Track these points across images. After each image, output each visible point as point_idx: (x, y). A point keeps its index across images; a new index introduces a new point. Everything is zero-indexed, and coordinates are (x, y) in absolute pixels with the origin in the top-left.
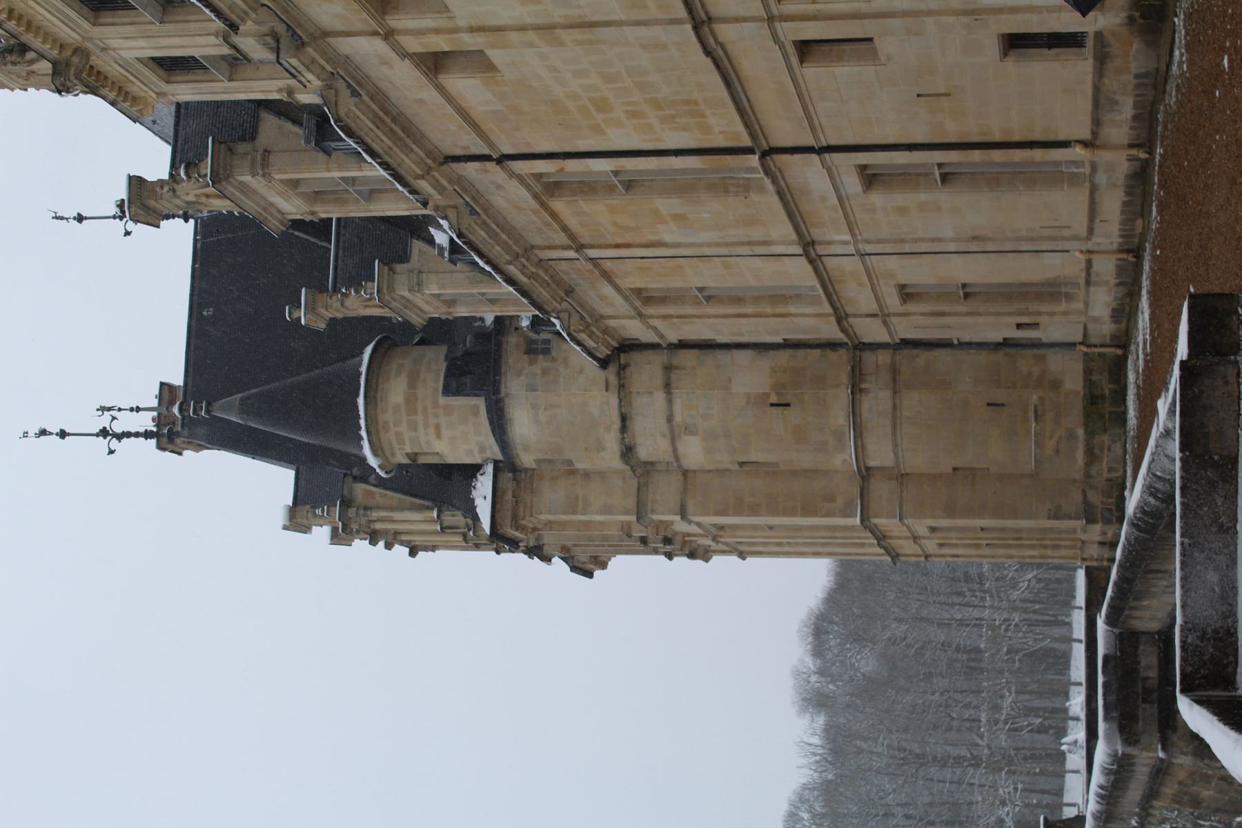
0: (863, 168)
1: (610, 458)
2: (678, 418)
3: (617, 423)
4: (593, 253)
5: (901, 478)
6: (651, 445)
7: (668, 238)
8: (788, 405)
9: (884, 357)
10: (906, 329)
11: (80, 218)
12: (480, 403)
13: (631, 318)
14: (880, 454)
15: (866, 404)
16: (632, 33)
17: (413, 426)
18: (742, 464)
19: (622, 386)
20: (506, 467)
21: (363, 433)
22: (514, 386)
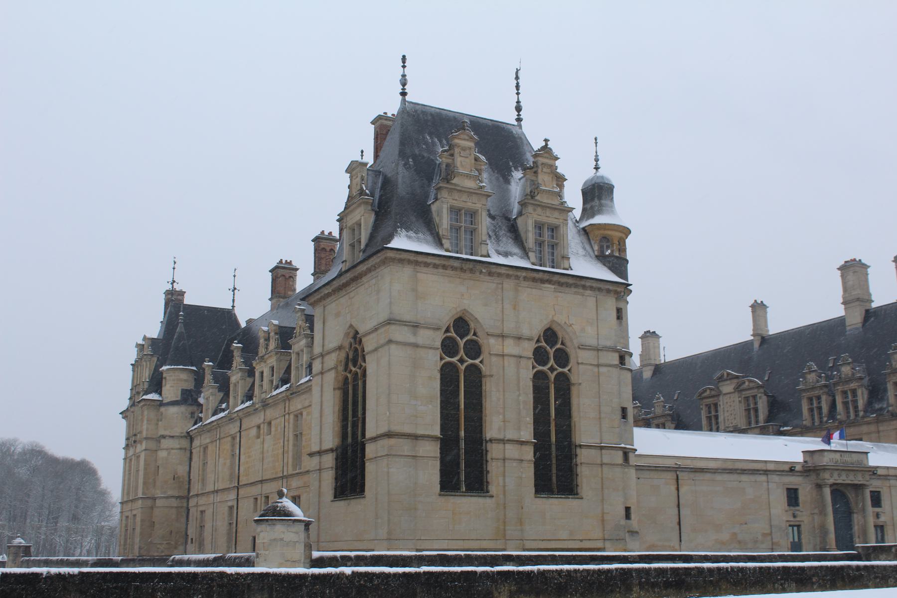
0: (233, 506)
1: (162, 432)
2: (173, 451)
3: (172, 435)
4: (218, 441)
5: (152, 508)
6: (165, 443)
7: (220, 460)
8: (174, 480)
9: (185, 505)
10: (193, 511)
11: (234, 276)
12: (179, 398)
13: (200, 443)
14: (159, 503)
15: (173, 500)
16: (261, 468)
17: (174, 380)
18: (158, 467)
19: (182, 437)
20: (161, 404)
21: (173, 367)
22: (182, 408)
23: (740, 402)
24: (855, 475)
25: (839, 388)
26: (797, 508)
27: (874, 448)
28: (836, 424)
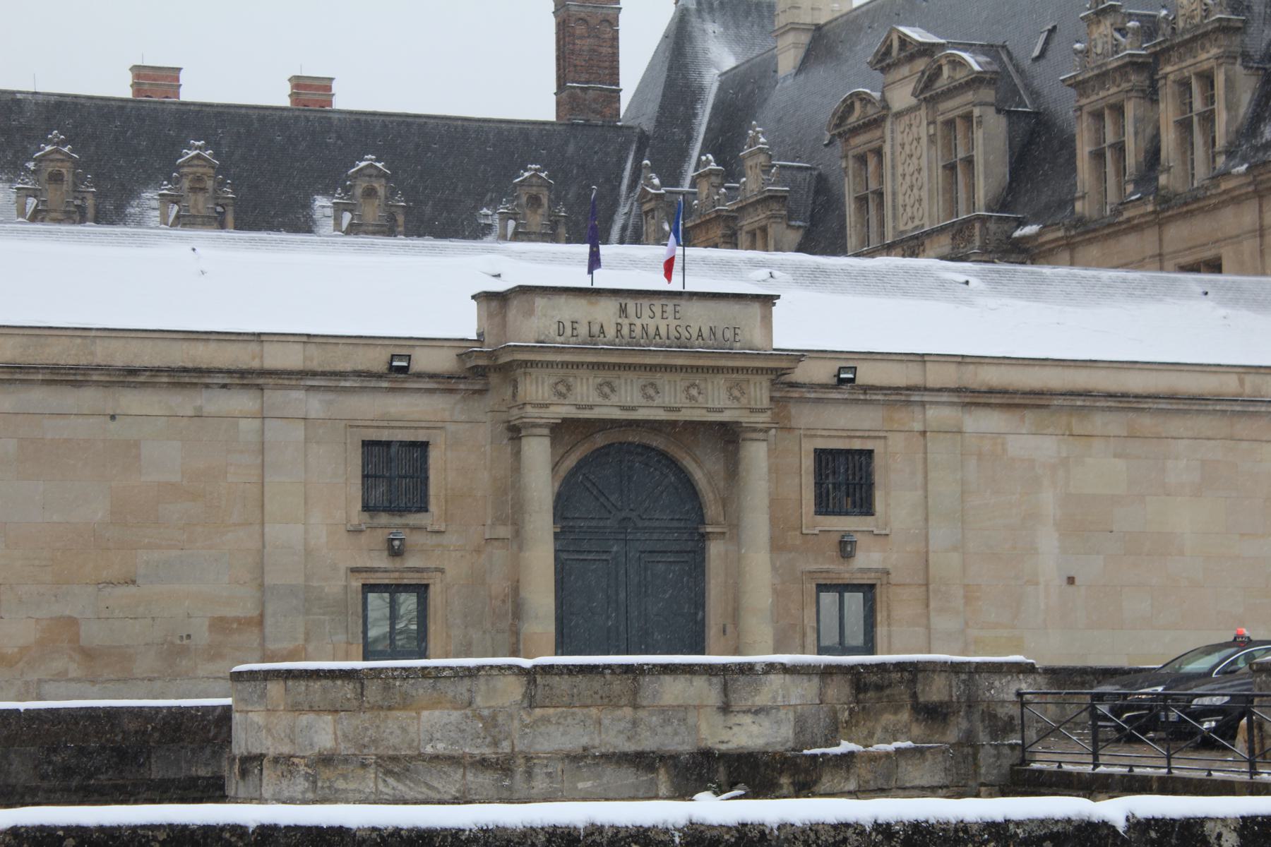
23: (932, 140)
24: (693, 385)
25: (1168, 69)
26: (414, 519)
27: (974, 282)
28: (1150, 208)
